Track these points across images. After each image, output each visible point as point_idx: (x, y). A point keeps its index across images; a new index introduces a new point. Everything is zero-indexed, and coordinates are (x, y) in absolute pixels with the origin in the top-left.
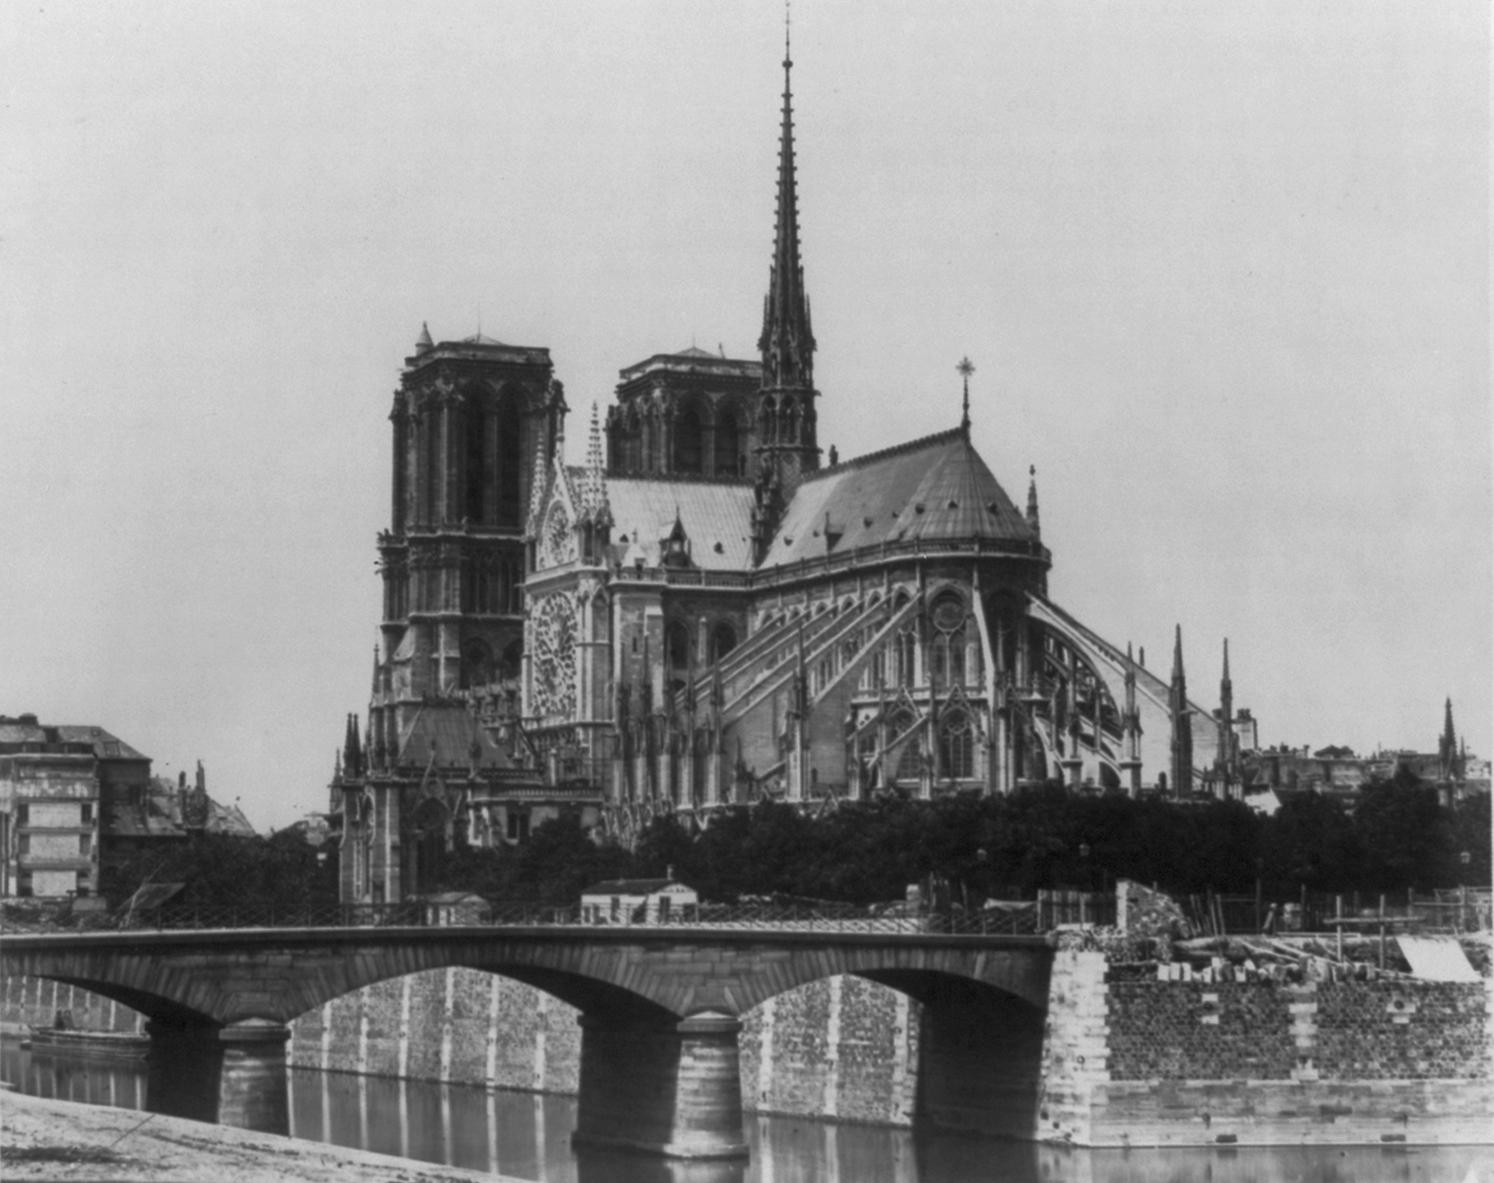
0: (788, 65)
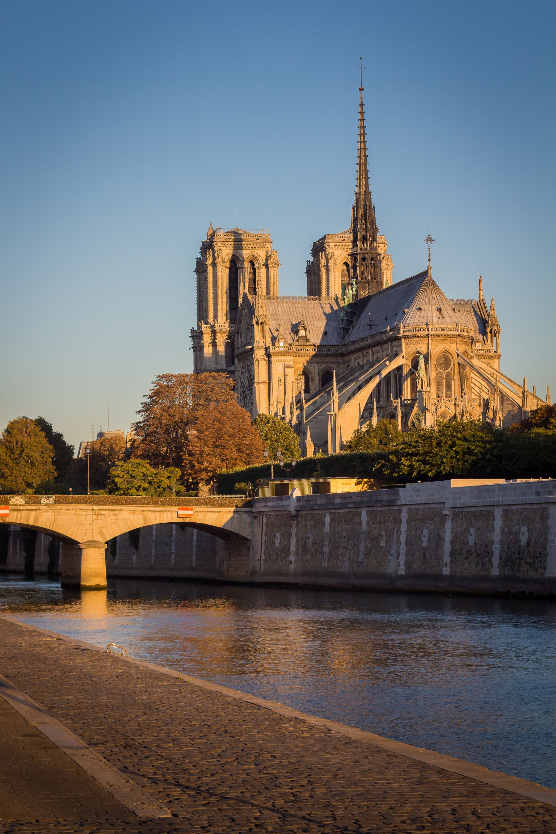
0: (362, 90)
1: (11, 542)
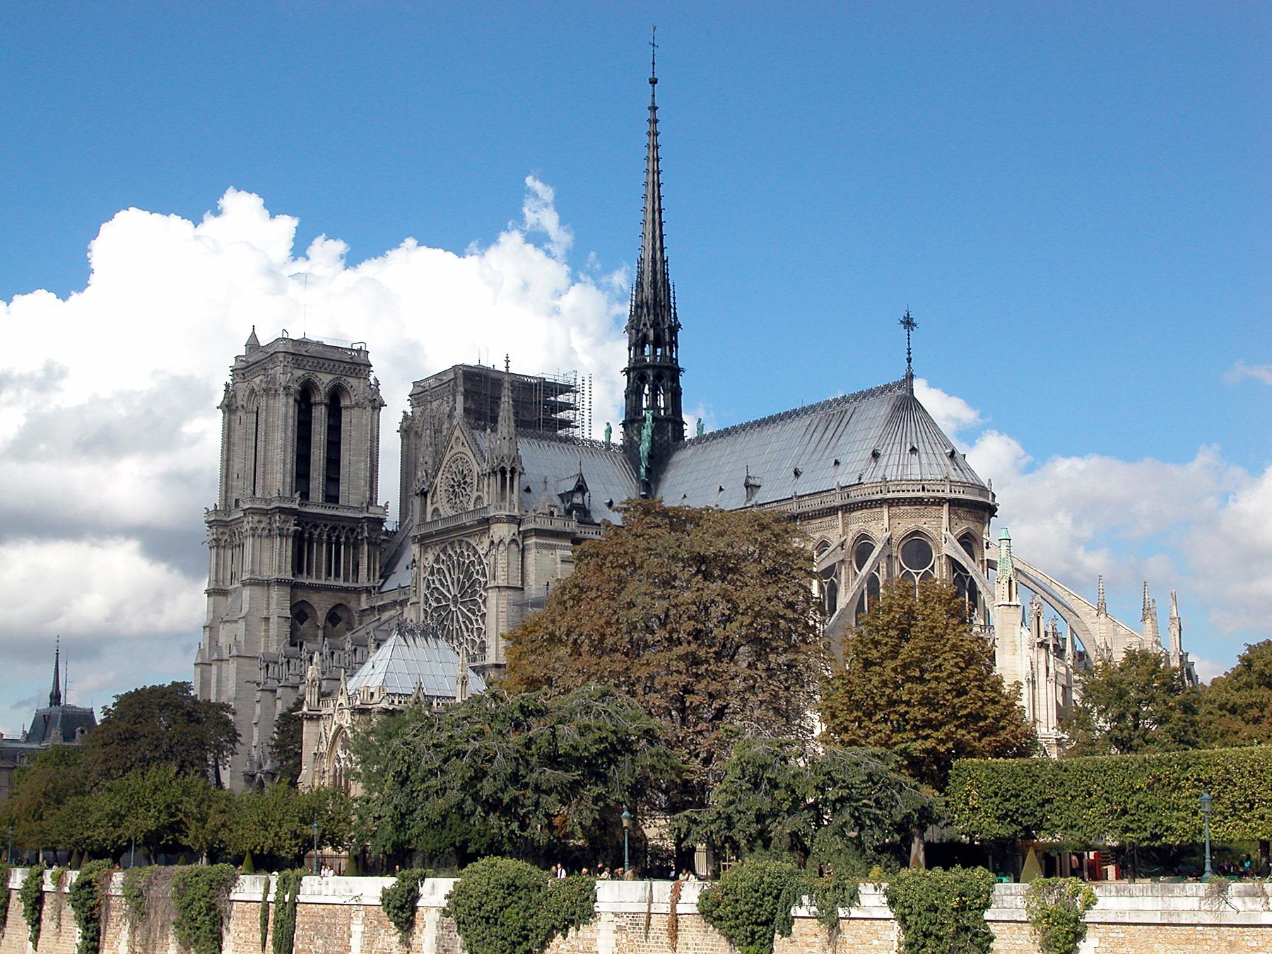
0: (654, 82)
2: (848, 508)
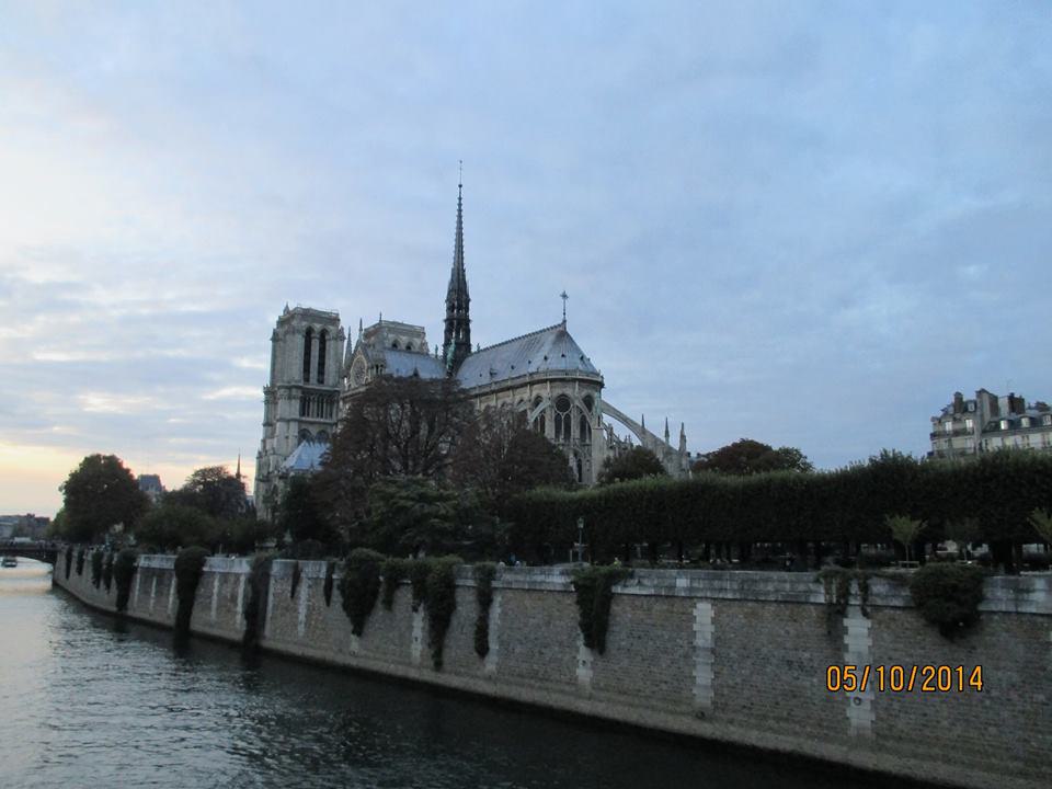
0: (460, 186)
1: (138, 580)
2: (532, 384)
